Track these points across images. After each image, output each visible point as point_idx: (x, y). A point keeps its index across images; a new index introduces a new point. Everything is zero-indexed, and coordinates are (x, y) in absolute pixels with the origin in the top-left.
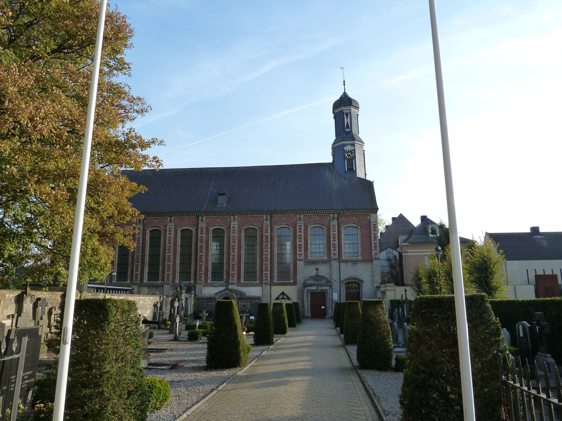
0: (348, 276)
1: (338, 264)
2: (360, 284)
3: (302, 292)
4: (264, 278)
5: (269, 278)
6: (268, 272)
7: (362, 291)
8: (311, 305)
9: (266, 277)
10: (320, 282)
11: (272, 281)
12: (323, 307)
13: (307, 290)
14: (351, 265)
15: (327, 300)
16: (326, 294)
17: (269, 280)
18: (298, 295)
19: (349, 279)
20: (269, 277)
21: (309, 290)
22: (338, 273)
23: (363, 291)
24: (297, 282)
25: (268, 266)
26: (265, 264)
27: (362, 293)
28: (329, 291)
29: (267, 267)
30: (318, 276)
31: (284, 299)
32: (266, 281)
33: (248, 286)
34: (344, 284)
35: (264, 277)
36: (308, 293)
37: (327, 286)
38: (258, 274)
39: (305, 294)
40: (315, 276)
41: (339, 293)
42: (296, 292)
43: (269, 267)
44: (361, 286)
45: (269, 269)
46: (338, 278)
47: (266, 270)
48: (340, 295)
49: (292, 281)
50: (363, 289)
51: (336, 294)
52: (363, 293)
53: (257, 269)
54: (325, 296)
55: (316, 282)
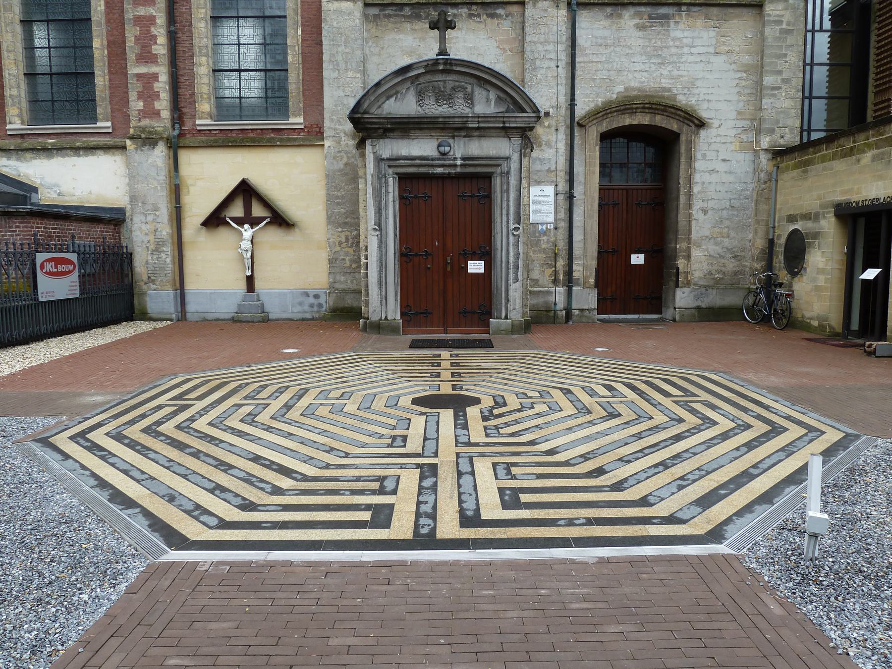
0: (620, 88)
1: (563, 12)
2: (683, 138)
3: (352, 176)
4: (136, 105)
5: (163, 105)
6: (154, 69)
7: (690, 179)
8: (405, 257)
9: (148, 95)
10: (460, 108)
11: (188, 126)
12: (476, 267)
13: (379, 160)
14: (641, 27)
15: (503, 223)
16: (497, 182)
17: (166, 114)
18: (331, 200)
19: (625, 106)
20: (165, 96)
21: (393, 161)
22: (563, 72)
23: (697, 178)
24: (327, 124)
25: (154, 31)
26: (138, 20)
27: (690, 189)
28: (514, 166)
29: (145, 41)
30: (450, 62)
31: (254, 222)
32: (145, 122)
33: (46, 151)
34: (594, 133)
35: (133, 95)
36: (381, 177)
37: (506, 131)
38: (101, 80)
39: (367, 188)
40: (432, 67)
41: (563, 186)
42: (323, 183)
43: (162, 40)
44: (689, 150)
45: (160, 47)
46: (563, 100)
47: (146, 57)
48: (570, 197)
49: (297, 121)
50: (699, 165)
51: (550, 190)
52: (696, 189)
53: (97, 54)
54: (488, 197)
55: (434, 109)
